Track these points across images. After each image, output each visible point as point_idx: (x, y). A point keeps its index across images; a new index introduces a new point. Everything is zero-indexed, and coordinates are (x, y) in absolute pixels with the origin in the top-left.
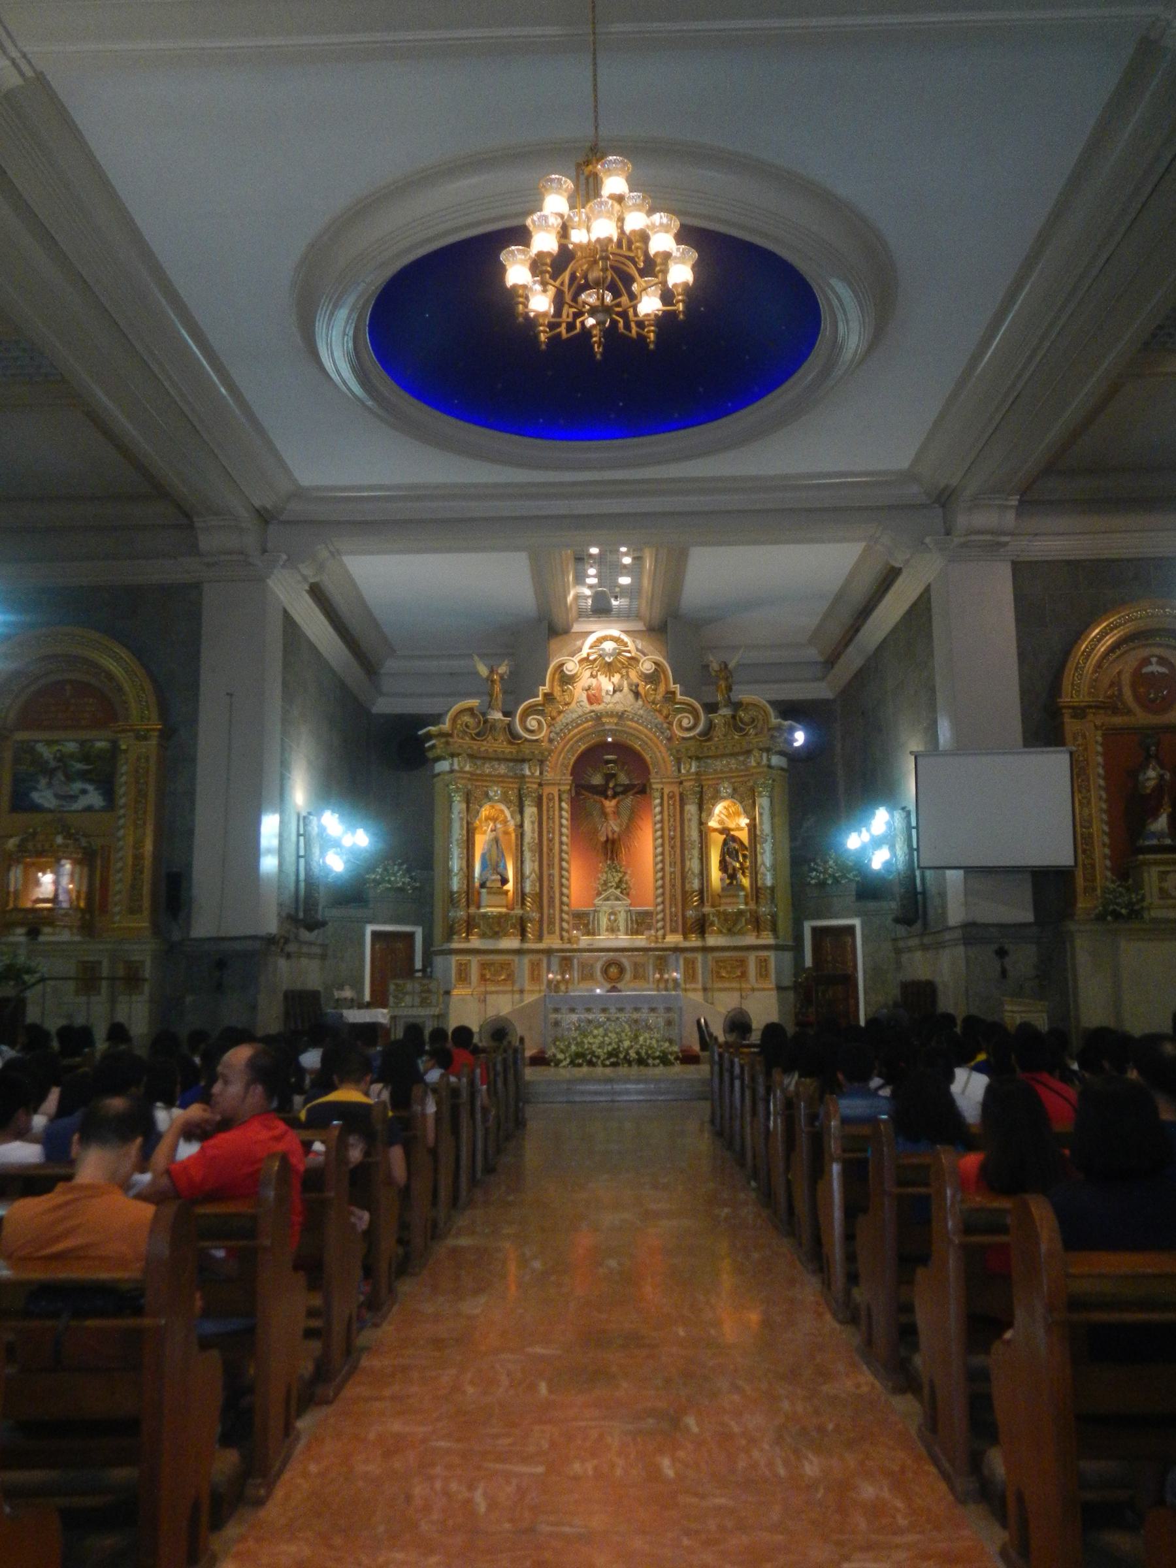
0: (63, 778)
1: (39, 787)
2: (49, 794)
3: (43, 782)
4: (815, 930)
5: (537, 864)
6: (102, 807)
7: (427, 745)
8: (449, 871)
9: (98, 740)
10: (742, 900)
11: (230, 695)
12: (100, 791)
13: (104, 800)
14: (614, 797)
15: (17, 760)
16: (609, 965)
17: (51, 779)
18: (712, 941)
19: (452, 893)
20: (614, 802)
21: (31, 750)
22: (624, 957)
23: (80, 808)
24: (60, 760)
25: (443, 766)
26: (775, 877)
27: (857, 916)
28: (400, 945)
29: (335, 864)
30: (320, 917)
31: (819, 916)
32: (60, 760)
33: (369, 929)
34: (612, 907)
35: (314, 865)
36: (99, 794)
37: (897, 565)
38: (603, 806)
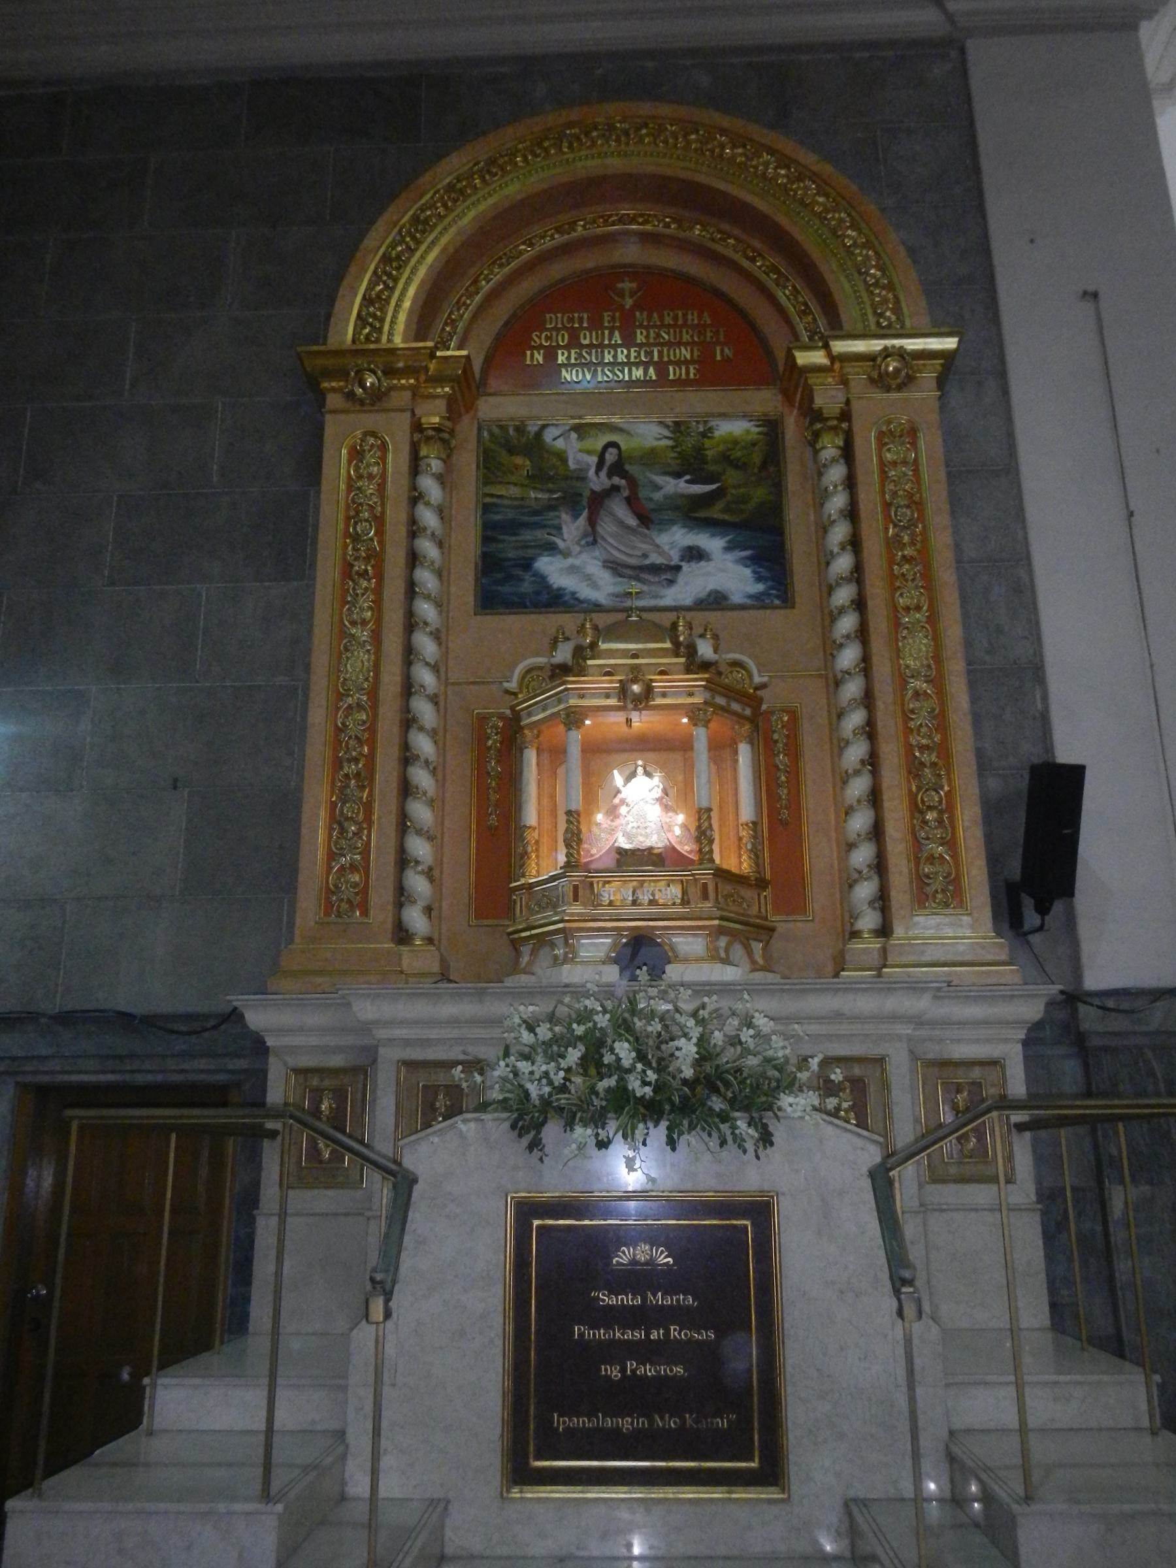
0: (632, 521)
1: (561, 544)
2: (592, 563)
3: (572, 528)
6: (757, 597)
9: (723, 416)
11: (1095, 295)
12: (748, 553)
13: (759, 579)
15: (490, 467)
17: (592, 522)
21: (534, 446)
23: (688, 602)
24: (617, 469)
32: (617, 469)
36: (743, 561)
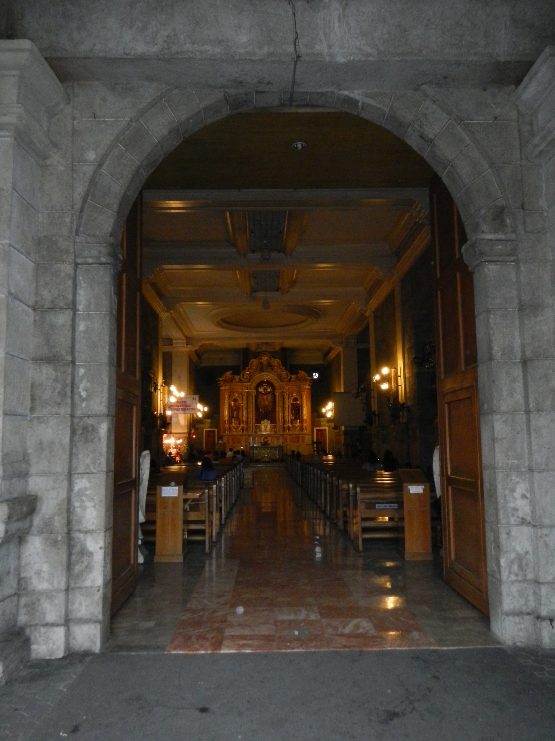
4: (317, 430)
10: (298, 423)
14: (266, 395)
16: (265, 438)
18: (291, 432)
19: (225, 421)
20: (266, 396)
25: (223, 388)
26: (308, 416)
27: (327, 426)
29: (200, 415)
31: (318, 426)
33: (205, 430)
34: (266, 424)
37: (333, 346)
38: (263, 399)
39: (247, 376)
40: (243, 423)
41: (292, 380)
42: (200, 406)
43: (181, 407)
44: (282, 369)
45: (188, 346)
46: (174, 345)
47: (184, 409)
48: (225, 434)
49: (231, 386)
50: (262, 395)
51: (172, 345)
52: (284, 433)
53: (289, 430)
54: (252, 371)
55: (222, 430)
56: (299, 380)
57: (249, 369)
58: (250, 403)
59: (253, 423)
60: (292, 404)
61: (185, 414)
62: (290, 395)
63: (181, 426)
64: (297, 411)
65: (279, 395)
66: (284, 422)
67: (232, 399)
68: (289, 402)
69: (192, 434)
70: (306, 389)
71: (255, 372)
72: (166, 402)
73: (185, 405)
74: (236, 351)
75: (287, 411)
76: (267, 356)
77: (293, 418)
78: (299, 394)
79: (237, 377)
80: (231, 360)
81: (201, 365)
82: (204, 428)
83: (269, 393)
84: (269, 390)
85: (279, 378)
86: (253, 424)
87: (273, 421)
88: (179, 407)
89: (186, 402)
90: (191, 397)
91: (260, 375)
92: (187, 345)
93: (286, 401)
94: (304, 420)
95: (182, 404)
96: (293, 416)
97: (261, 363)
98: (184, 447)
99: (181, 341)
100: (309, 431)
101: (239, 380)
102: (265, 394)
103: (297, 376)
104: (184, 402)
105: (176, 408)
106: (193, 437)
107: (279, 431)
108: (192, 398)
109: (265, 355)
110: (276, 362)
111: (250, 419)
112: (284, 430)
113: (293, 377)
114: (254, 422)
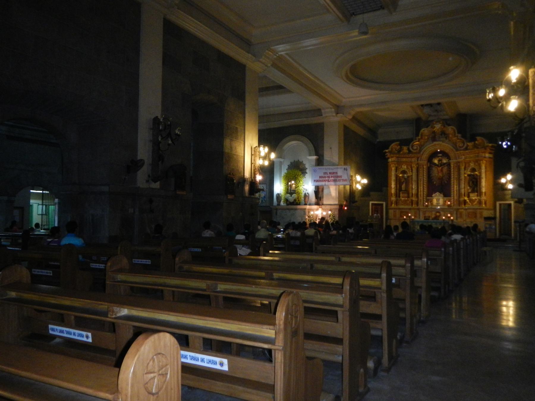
4: (500, 205)
5: (416, 186)
7: (386, 154)
8: (391, 188)
14: (441, 166)
18: (467, 206)
19: (392, 194)
20: (440, 168)
22: (441, 211)
28: (379, 207)
29: (359, 187)
30: (356, 200)
33: (371, 203)
35: (354, 187)
39: (417, 147)
40: (412, 196)
41: (469, 148)
42: (358, 178)
43: (333, 179)
44: (457, 136)
45: (338, 115)
46: (324, 115)
47: (335, 180)
48: (391, 207)
49: (397, 157)
50: (436, 167)
51: (322, 115)
52: (460, 208)
53: (465, 205)
54: (422, 140)
55: (389, 202)
56: (477, 148)
57: (419, 139)
58: (421, 175)
59: (423, 196)
60: (469, 175)
61: (335, 185)
62: (467, 165)
63: (333, 198)
64: (475, 183)
65: (453, 166)
66: (460, 195)
67: (400, 172)
68: (465, 174)
69: (344, 206)
70: (485, 157)
71: (426, 142)
72: (256, 165)
73: (336, 176)
74: (405, 122)
75: (462, 182)
76: (440, 124)
77: (470, 191)
78: (477, 164)
79: (405, 149)
80: (406, 132)
81: (378, 140)
82: (372, 200)
83: (444, 164)
84: (445, 161)
85: (454, 148)
86: (425, 198)
87: (447, 194)
88: (330, 178)
89: (337, 172)
90: (342, 168)
91: (432, 144)
92: (337, 114)
93: (462, 171)
94: (482, 192)
95: (332, 175)
96: (470, 189)
97: (434, 132)
98: (331, 219)
99: (328, 110)
100: (489, 205)
101: (407, 151)
102: (439, 165)
103: (475, 143)
104: (335, 173)
105: (327, 179)
106: (344, 209)
107: (454, 205)
108: (344, 168)
109: (438, 123)
110: (450, 130)
111: (421, 191)
112: (459, 203)
113: (470, 144)
114: (425, 195)
